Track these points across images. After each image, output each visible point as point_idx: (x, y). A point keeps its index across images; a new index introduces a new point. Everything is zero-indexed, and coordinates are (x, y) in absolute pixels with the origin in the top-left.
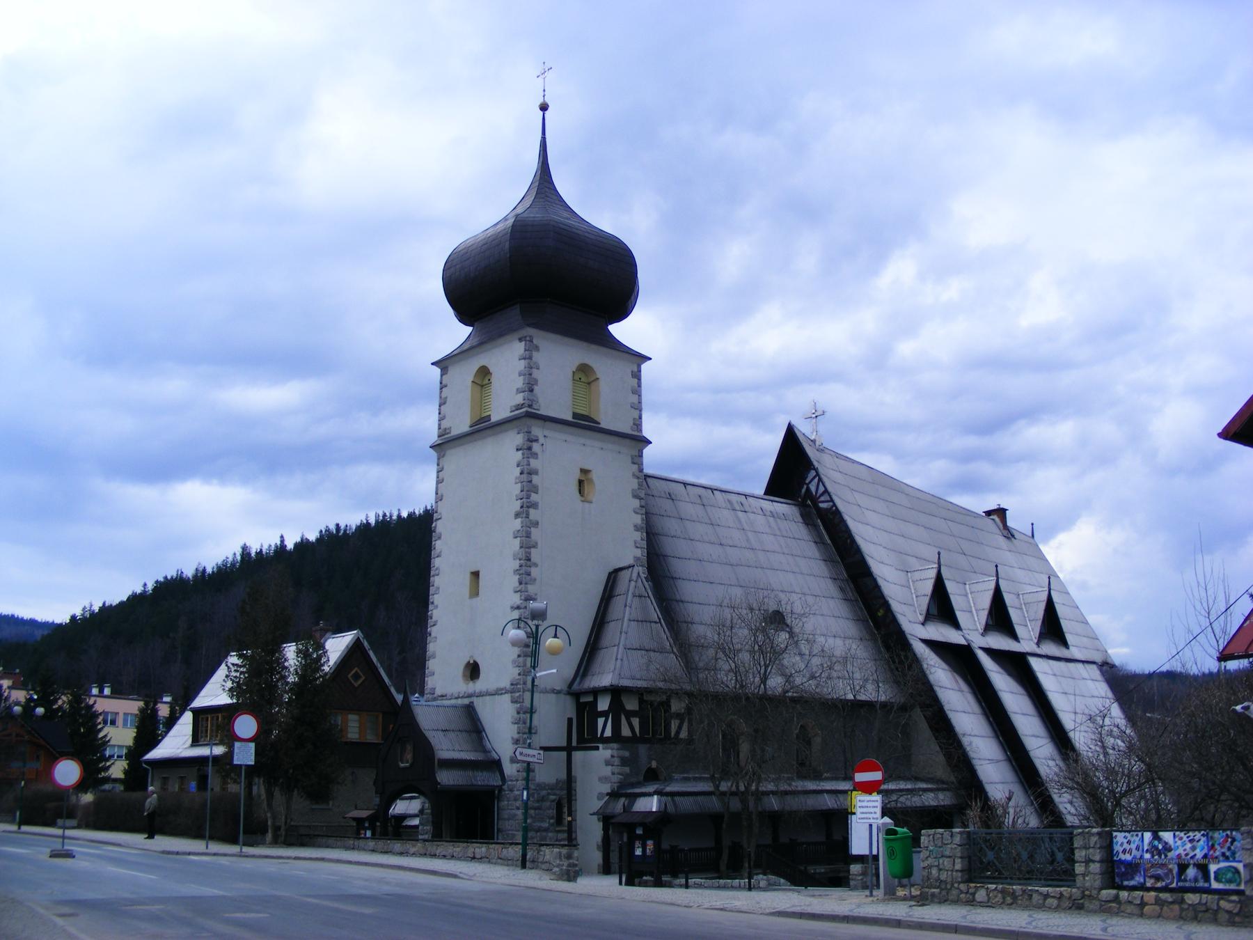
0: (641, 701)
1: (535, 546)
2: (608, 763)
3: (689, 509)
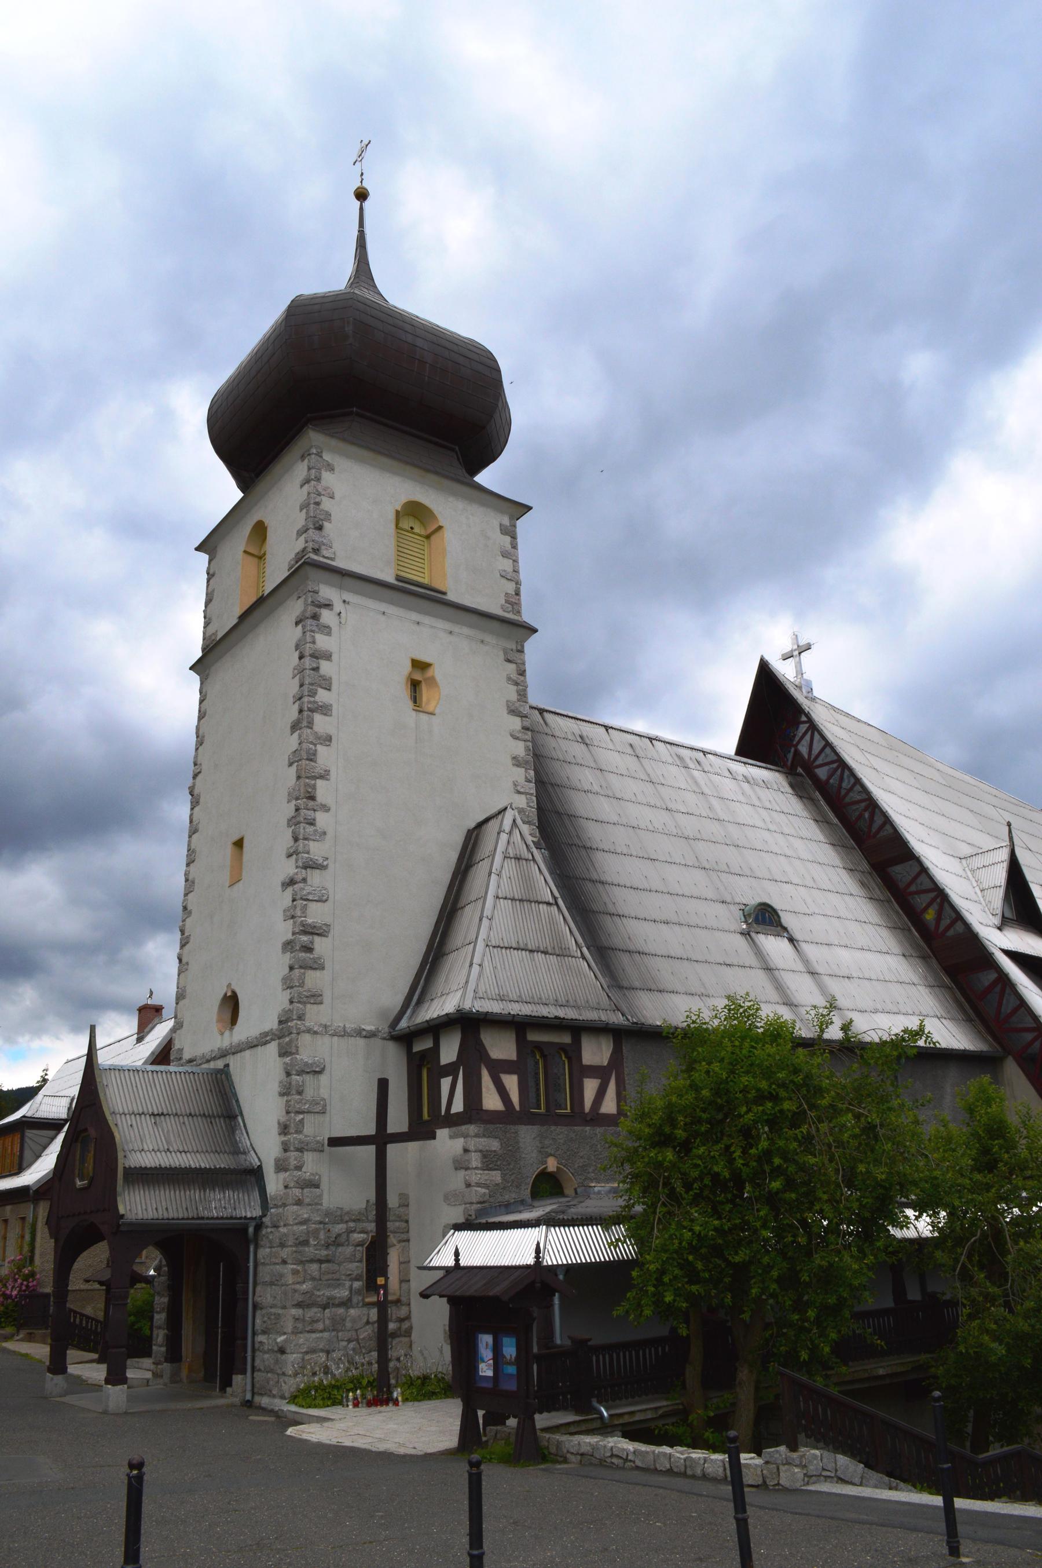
0: (521, 1042)
1: (324, 776)
3: (612, 759)
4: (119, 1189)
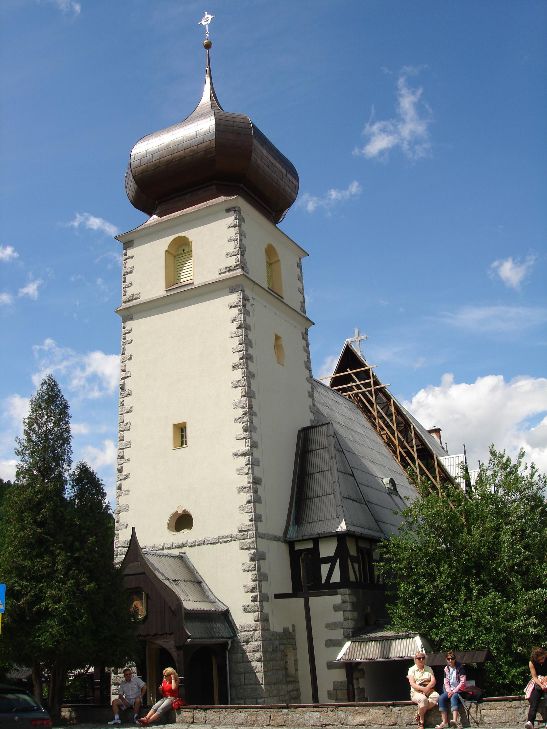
2: (337, 608)
4: (184, 621)
